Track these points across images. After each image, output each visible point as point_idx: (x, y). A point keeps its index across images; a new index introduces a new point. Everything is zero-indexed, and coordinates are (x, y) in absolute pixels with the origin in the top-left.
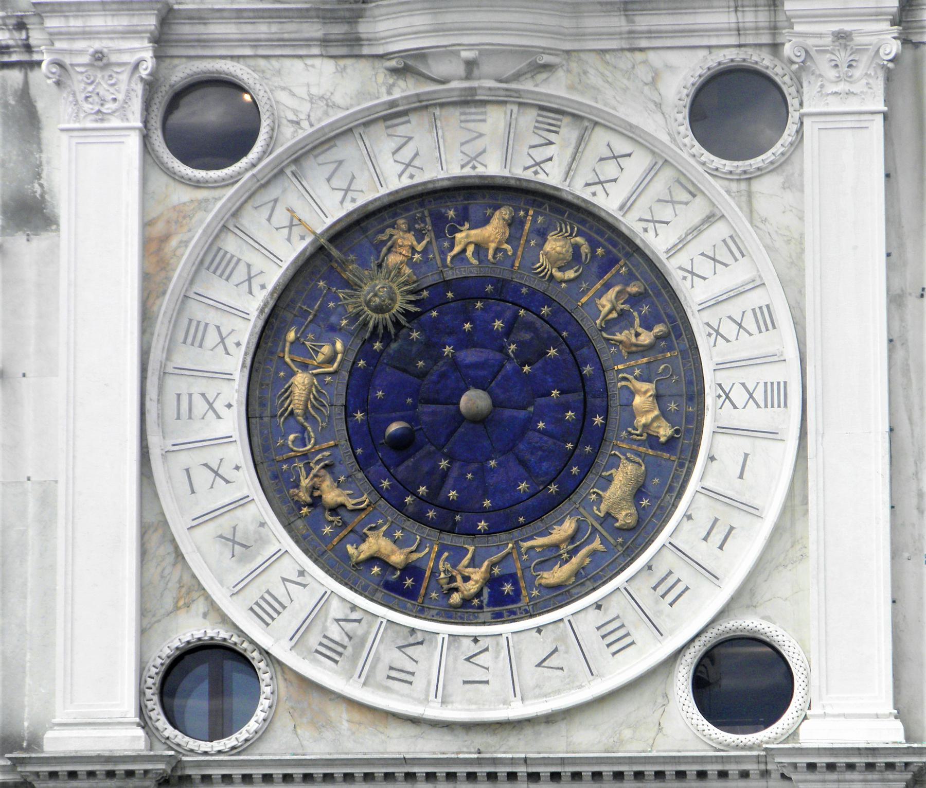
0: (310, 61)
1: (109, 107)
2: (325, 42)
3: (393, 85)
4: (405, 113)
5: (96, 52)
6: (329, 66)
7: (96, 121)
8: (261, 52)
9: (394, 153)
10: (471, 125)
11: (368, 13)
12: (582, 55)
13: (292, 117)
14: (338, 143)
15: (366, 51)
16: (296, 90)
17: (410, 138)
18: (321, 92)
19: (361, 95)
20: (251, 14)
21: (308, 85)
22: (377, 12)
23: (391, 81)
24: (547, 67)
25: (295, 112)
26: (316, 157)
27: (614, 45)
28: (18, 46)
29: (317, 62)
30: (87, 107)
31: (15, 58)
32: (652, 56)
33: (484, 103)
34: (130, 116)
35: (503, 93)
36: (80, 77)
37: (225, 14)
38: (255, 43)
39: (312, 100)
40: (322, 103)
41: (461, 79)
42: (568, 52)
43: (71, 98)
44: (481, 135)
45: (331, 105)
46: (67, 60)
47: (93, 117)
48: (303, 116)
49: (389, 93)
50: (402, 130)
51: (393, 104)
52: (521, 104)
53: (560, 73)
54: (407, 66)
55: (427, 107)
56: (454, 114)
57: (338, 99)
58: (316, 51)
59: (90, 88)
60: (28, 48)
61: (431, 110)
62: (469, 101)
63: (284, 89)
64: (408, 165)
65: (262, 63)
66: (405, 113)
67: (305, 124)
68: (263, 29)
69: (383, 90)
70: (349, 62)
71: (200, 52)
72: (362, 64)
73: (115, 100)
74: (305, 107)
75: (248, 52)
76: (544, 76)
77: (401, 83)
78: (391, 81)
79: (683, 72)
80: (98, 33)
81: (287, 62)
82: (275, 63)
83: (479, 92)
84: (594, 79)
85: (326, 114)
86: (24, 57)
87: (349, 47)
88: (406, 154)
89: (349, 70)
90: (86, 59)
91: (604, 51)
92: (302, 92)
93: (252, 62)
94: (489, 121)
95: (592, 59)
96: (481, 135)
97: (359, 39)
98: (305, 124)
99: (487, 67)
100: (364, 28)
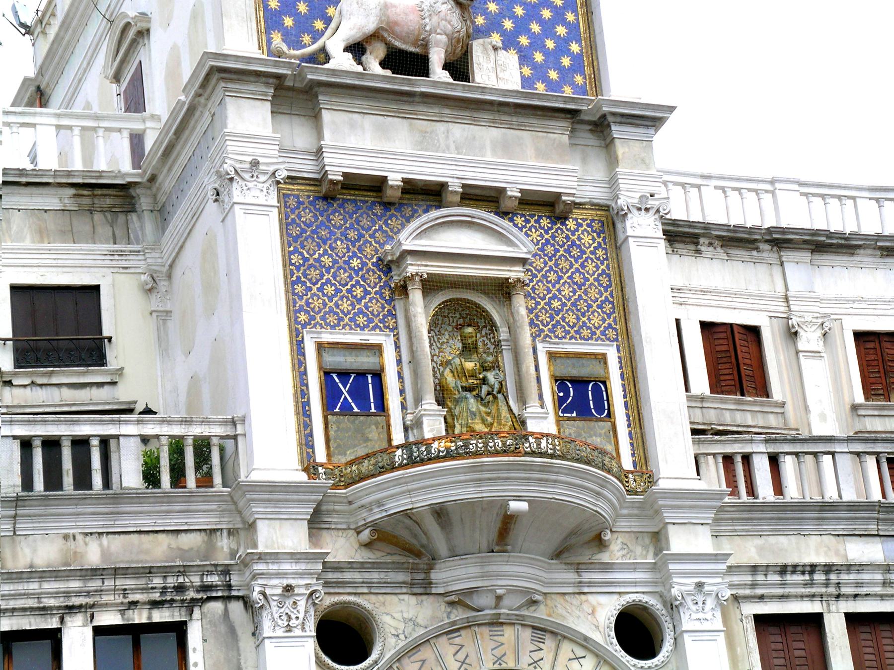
0: (401, 597)
1: (293, 622)
2: (412, 585)
3: (450, 613)
4: (458, 630)
5: (287, 586)
6: (413, 600)
7: (287, 631)
8: (373, 591)
9: (454, 655)
10: (496, 638)
11: (437, 566)
12: (553, 596)
13: (394, 632)
14: (422, 648)
15: (434, 591)
16: (394, 615)
17: (462, 646)
18: (410, 616)
19: (433, 618)
20: (369, 566)
21: (402, 612)
22: (443, 565)
23: (449, 610)
24: (535, 602)
25: (396, 629)
26: (409, 658)
27: (570, 590)
28: (223, 586)
29: (406, 597)
30: (280, 622)
31: (220, 594)
32: (590, 598)
33: (502, 624)
34: (307, 628)
35: (515, 617)
36: (275, 603)
37: (354, 566)
38: (369, 584)
39: (405, 621)
40: (411, 624)
41: (491, 609)
42: (545, 594)
43: (270, 617)
44: (502, 644)
45: (416, 625)
46: (268, 592)
47: (284, 629)
48: (400, 632)
49: (449, 618)
50: (457, 641)
51: (454, 623)
52: (523, 625)
53: (542, 607)
54: (459, 600)
55: (470, 626)
56: (485, 630)
57: (420, 621)
58: (404, 590)
59: (282, 610)
60: (229, 587)
61: (473, 628)
62: (496, 623)
63: (387, 614)
64: (463, 663)
65: (373, 597)
66: (458, 630)
67: (402, 637)
68: (375, 576)
69: (445, 615)
70: (424, 597)
71: (337, 590)
72: (431, 597)
73: (297, 618)
74: (401, 626)
75: (366, 590)
76: (533, 608)
77: (454, 611)
78: (449, 610)
79: (607, 609)
80: (286, 574)
81: (388, 597)
82: (380, 597)
83: (502, 616)
84: (560, 610)
85: (414, 630)
86: (226, 594)
87: (422, 587)
88: (461, 656)
89: (425, 603)
90: (279, 591)
91: (564, 594)
92: (398, 616)
93: (367, 597)
94: (506, 635)
95: (559, 599)
96: (502, 644)
97: (431, 583)
98: (402, 637)
99: (506, 602)
100: (435, 576)
